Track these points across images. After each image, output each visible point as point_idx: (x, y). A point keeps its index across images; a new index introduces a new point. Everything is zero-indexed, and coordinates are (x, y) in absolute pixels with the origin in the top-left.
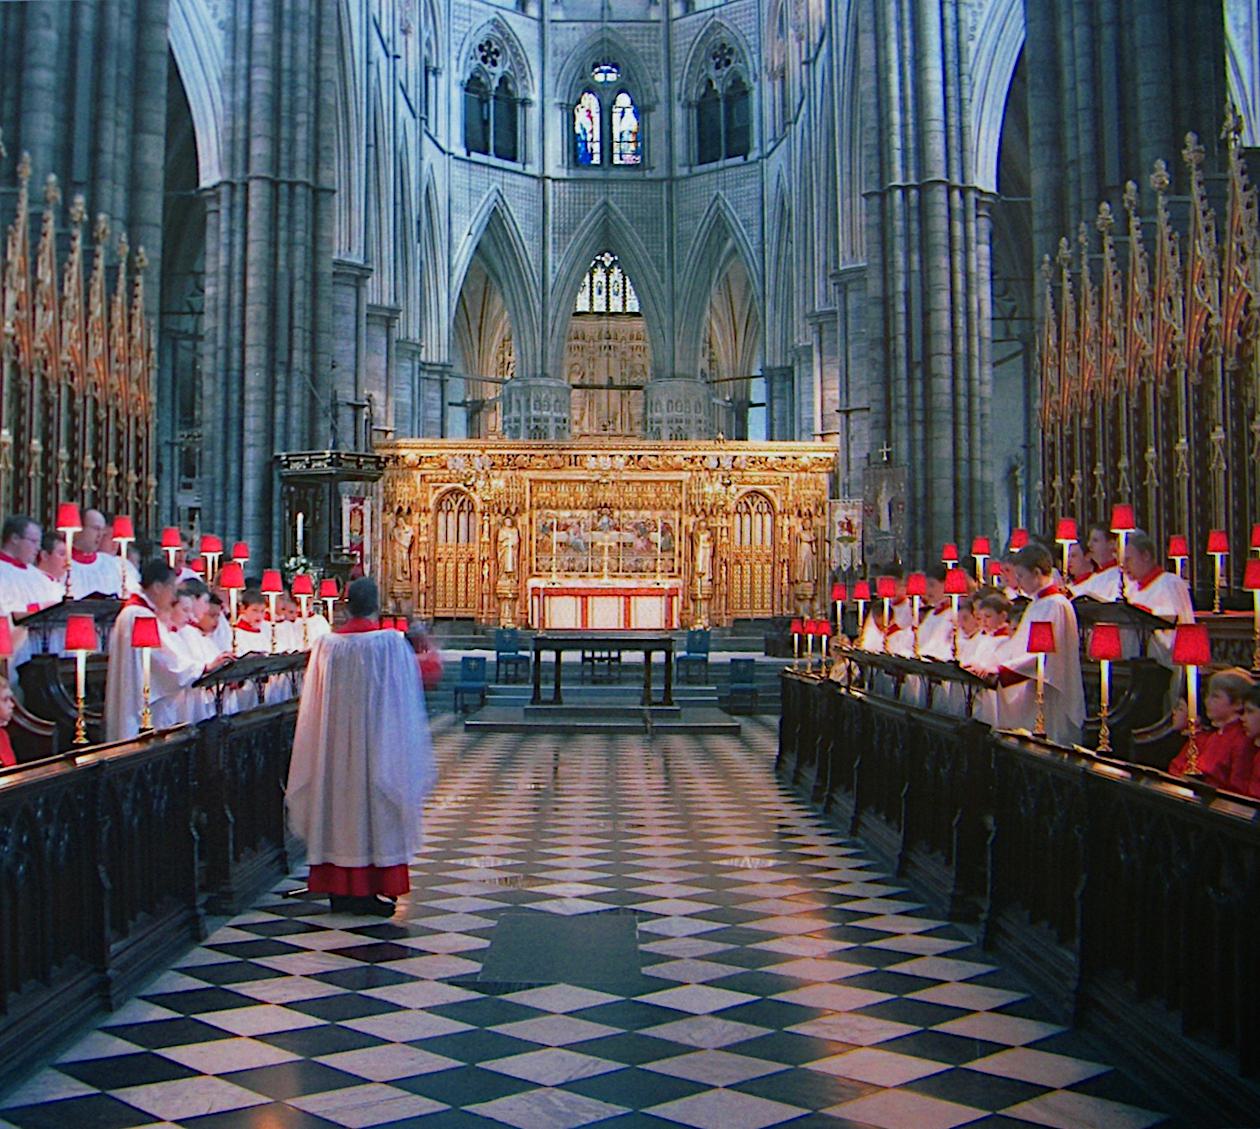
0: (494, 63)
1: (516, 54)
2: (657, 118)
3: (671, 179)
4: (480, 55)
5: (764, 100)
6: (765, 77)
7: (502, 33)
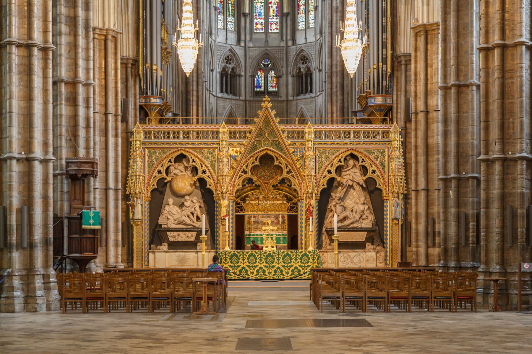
0: (230, 63)
1: (237, 60)
2: (283, 80)
3: (287, 101)
5: (317, 77)
6: (317, 70)
7: (232, 53)
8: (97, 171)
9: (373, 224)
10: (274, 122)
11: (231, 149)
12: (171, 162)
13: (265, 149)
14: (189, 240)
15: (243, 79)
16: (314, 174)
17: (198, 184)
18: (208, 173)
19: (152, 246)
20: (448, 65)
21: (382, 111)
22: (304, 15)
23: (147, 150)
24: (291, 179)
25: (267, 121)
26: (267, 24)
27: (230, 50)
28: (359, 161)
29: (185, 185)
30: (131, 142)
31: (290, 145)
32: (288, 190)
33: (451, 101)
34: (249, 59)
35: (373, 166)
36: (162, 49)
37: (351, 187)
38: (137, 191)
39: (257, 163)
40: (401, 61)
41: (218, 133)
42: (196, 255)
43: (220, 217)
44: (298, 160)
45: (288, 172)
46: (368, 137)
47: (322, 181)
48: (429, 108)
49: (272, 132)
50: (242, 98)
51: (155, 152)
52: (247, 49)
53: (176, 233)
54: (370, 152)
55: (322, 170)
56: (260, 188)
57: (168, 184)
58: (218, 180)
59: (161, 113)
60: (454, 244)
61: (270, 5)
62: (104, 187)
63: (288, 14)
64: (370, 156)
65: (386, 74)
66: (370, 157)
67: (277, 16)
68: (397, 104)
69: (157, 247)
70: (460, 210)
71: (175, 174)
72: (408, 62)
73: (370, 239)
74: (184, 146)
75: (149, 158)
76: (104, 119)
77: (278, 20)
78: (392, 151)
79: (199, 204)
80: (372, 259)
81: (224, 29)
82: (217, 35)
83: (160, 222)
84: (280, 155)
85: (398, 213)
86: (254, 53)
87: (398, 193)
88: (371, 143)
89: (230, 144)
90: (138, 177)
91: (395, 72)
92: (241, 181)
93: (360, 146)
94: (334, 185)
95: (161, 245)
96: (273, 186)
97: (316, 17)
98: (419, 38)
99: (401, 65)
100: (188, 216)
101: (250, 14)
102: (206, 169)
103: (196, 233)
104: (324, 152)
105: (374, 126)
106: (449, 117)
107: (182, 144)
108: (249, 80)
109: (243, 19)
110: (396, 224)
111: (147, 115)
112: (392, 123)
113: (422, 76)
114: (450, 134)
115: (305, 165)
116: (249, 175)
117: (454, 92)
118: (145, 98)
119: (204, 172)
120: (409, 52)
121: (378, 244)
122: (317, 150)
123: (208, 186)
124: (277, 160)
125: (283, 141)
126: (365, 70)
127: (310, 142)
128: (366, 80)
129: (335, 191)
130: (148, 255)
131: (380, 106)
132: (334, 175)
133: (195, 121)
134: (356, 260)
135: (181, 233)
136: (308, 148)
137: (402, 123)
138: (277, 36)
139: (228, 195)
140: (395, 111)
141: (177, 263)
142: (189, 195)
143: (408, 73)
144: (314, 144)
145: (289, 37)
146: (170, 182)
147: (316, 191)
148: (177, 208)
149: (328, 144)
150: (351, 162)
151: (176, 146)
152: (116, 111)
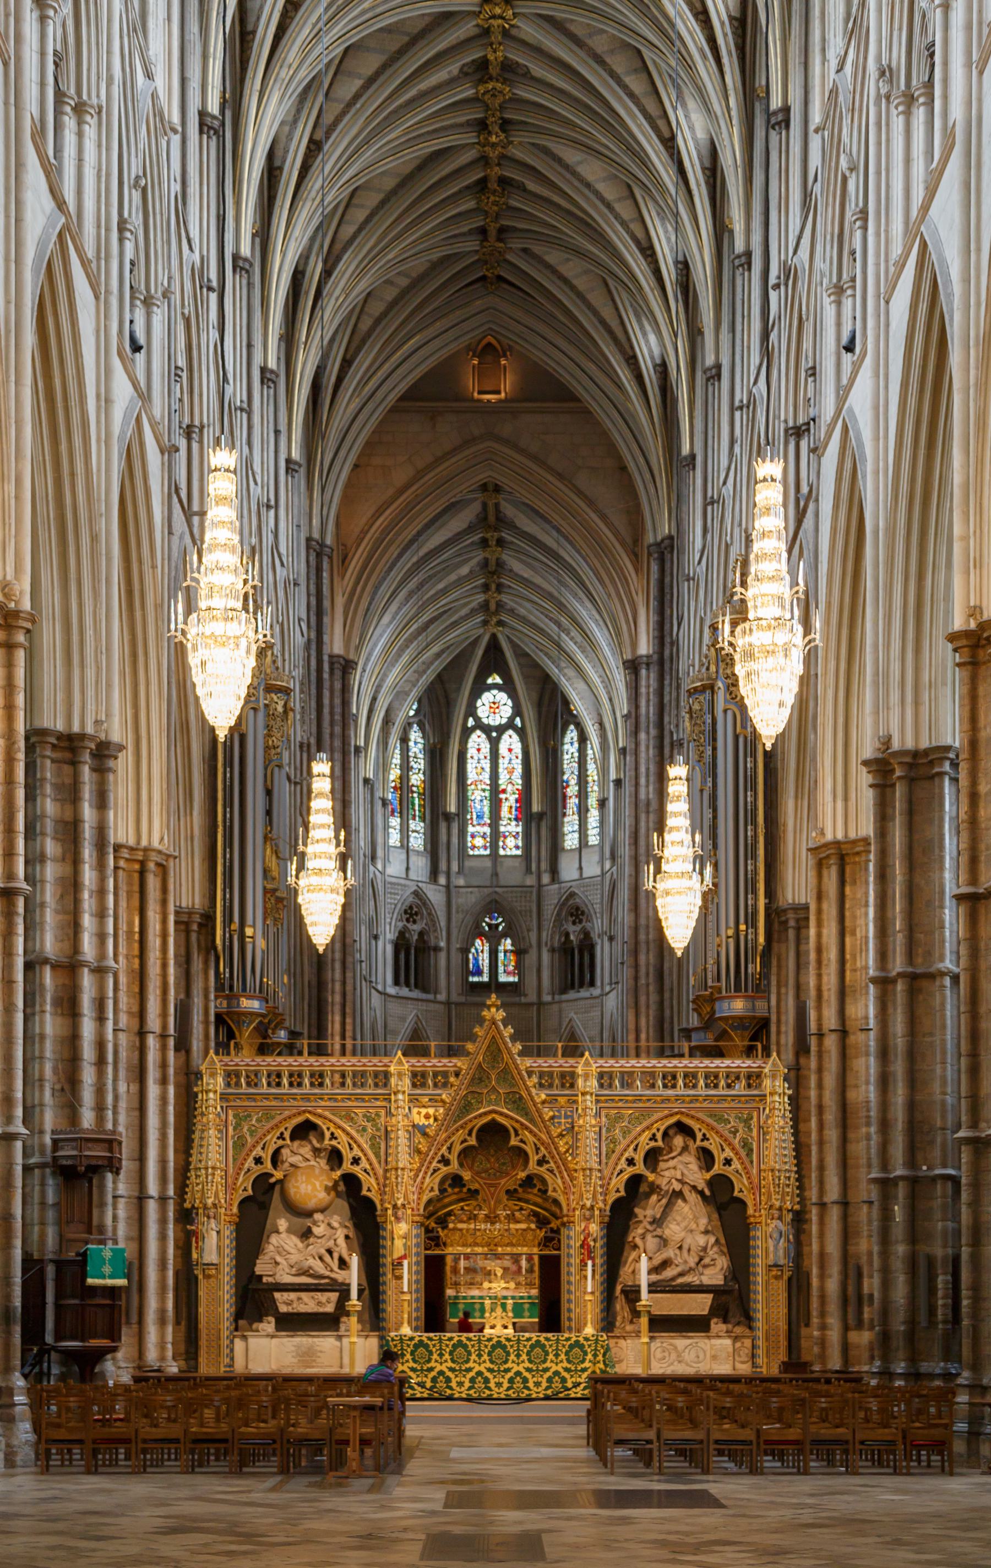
0: (415, 922)
1: (430, 914)
2: (531, 958)
3: (540, 1004)
4: (405, 917)
5: (604, 953)
6: (606, 939)
8: (120, 1160)
9: (725, 1277)
10: (510, 1053)
11: (415, 1110)
12: (284, 1139)
14: (321, 1310)
15: (442, 956)
16: (596, 1166)
17: (342, 1187)
18: (364, 1163)
19: (241, 1322)
20: (890, 932)
21: (744, 1028)
22: (576, 817)
23: (230, 1112)
24: (546, 1177)
25: (495, 1051)
26: (496, 836)
27: (416, 893)
28: (694, 1138)
29: (314, 1188)
30: (196, 1095)
31: (544, 1102)
32: (539, 1200)
33: (895, 1009)
34: (457, 912)
35: (727, 1149)
36: (266, 891)
37: (678, 1195)
38: (210, 1201)
39: (473, 1141)
40: (786, 922)
41: (387, 1075)
42: (338, 1343)
43: (389, 1259)
44: (561, 1135)
45: (541, 1162)
46: (716, 1086)
47: (614, 1181)
48: (848, 1023)
49: (506, 1075)
50: (442, 997)
51: (249, 1116)
52: (453, 890)
53: (293, 1296)
54: (721, 1120)
55: (614, 1157)
56: (480, 1197)
57: (277, 1188)
58: (386, 1178)
59: (263, 1030)
60: (904, 1323)
61: (502, 796)
62: (136, 1194)
63: (541, 816)
64: (719, 1127)
65: (755, 947)
66: (721, 1130)
67: (517, 819)
68: (778, 1013)
69: (251, 1324)
70: (917, 1247)
71: (292, 1165)
72: (803, 923)
73: (721, 1311)
74: (313, 1104)
75: (235, 1129)
76: (138, 1044)
77: (520, 829)
78: (768, 1117)
79: (345, 1231)
80: (724, 1355)
81: (402, 846)
82: (386, 860)
83: (258, 1270)
84: (522, 1124)
85: (781, 1253)
86: (468, 899)
87: (780, 1209)
88: (723, 1098)
89: (414, 1100)
91: (775, 946)
92: (437, 1180)
93: (698, 1105)
94: (641, 1190)
95: (261, 1321)
96: (508, 1192)
97: (602, 822)
98: (825, 872)
99: (786, 930)
100: (321, 1258)
101: (458, 815)
102: (360, 1154)
103: (337, 1294)
104: (619, 1118)
105: (727, 1062)
106: (891, 1043)
107: (309, 1100)
108: (456, 958)
109: (443, 826)
110: (776, 1277)
111: (231, 1035)
112: (769, 1056)
113: (832, 954)
114: (895, 1081)
115: (577, 1147)
116: (454, 1166)
117: (903, 991)
118: (228, 998)
119: (356, 1161)
120: (803, 901)
121: (737, 1320)
122: (603, 1113)
123: (364, 1192)
124: (517, 1134)
125: (530, 1095)
126: (709, 939)
127: (588, 1097)
128: (711, 961)
129: (643, 1203)
130: (232, 1342)
131: (741, 1018)
132: (640, 1168)
133: (337, 1047)
134: (689, 1356)
135: (303, 1295)
136: (584, 1110)
137: (789, 1056)
138: (517, 863)
139: (409, 1212)
140: (773, 1028)
141: (295, 1360)
142: (322, 1211)
143: (803, 947)
144: (597, 1101)
145: (544, 865)
146: (280, 1182)
147: (601, 1205)
148: (296, 1240)
149: (627, 1101)
150: (678, 1141)
151: (296, 1103)
152: (164, 1026)
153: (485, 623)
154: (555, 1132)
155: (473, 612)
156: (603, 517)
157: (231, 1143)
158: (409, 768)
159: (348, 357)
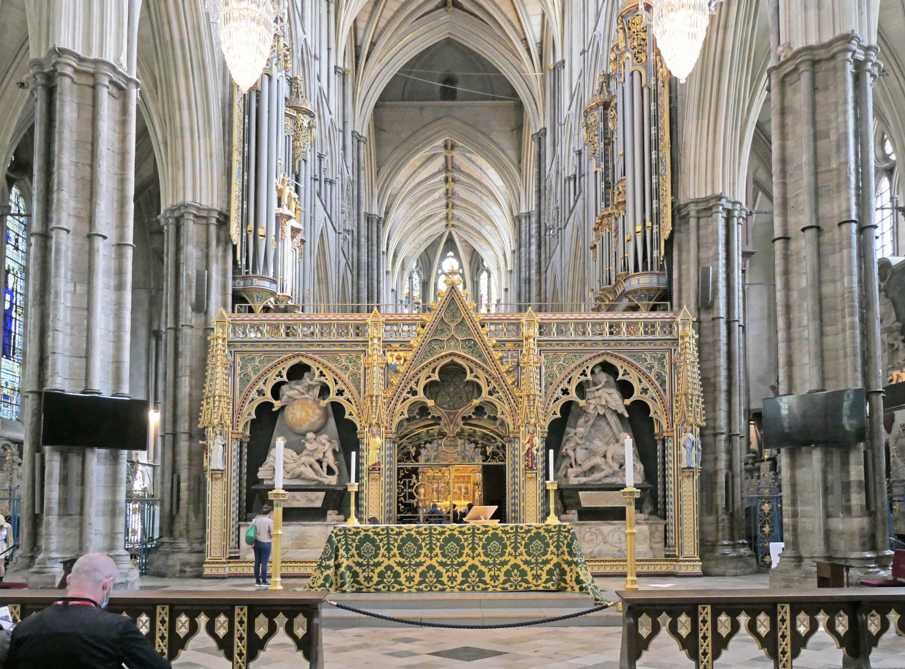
11: (388, 354)
12: (282, 377)
13: (450, 355)
18: (347, 394)
35: (644, 381)
38: (216, 422)
39: (436, 377)
44: (508, 372)
45: (490, 393)
51: (253, 359)
55: (551, 388)
66: (639, 366)
71: (289, 397)
75: (242, 368)
90: (217, 398)
104: (557, 358)
119: (340, 393)
132: (573, 396)
150: (603, 377)
153: (447, 225)
154: (503, 369)
155: (441, 220)
156: (503, 151)
157: (238, 380)
158: (413, 289)
159: (374, 41)
